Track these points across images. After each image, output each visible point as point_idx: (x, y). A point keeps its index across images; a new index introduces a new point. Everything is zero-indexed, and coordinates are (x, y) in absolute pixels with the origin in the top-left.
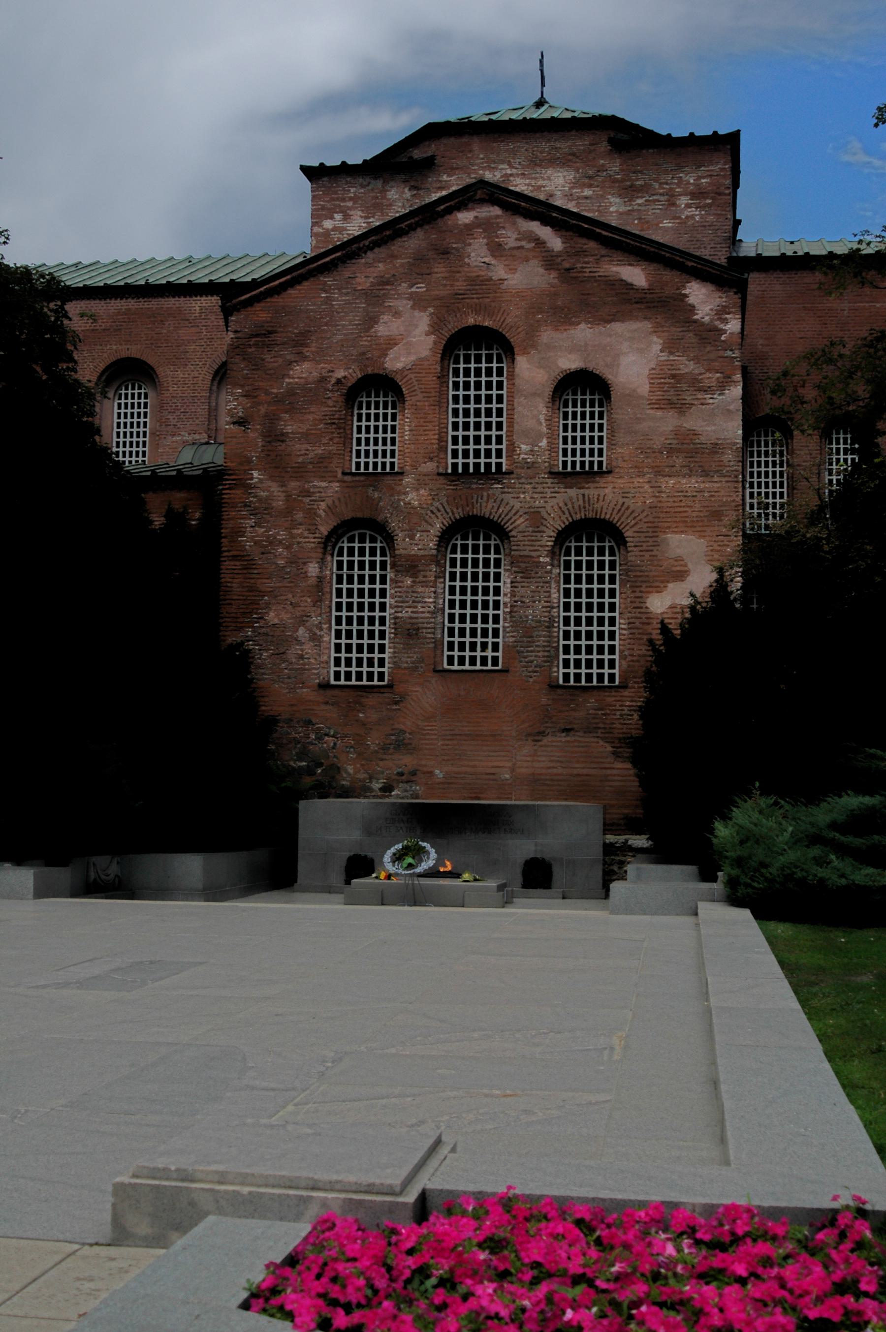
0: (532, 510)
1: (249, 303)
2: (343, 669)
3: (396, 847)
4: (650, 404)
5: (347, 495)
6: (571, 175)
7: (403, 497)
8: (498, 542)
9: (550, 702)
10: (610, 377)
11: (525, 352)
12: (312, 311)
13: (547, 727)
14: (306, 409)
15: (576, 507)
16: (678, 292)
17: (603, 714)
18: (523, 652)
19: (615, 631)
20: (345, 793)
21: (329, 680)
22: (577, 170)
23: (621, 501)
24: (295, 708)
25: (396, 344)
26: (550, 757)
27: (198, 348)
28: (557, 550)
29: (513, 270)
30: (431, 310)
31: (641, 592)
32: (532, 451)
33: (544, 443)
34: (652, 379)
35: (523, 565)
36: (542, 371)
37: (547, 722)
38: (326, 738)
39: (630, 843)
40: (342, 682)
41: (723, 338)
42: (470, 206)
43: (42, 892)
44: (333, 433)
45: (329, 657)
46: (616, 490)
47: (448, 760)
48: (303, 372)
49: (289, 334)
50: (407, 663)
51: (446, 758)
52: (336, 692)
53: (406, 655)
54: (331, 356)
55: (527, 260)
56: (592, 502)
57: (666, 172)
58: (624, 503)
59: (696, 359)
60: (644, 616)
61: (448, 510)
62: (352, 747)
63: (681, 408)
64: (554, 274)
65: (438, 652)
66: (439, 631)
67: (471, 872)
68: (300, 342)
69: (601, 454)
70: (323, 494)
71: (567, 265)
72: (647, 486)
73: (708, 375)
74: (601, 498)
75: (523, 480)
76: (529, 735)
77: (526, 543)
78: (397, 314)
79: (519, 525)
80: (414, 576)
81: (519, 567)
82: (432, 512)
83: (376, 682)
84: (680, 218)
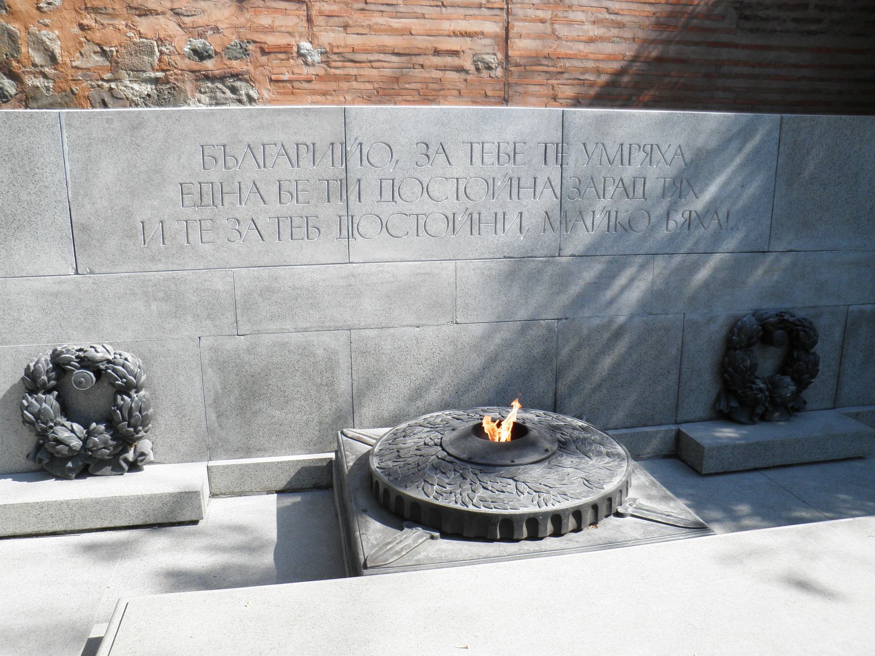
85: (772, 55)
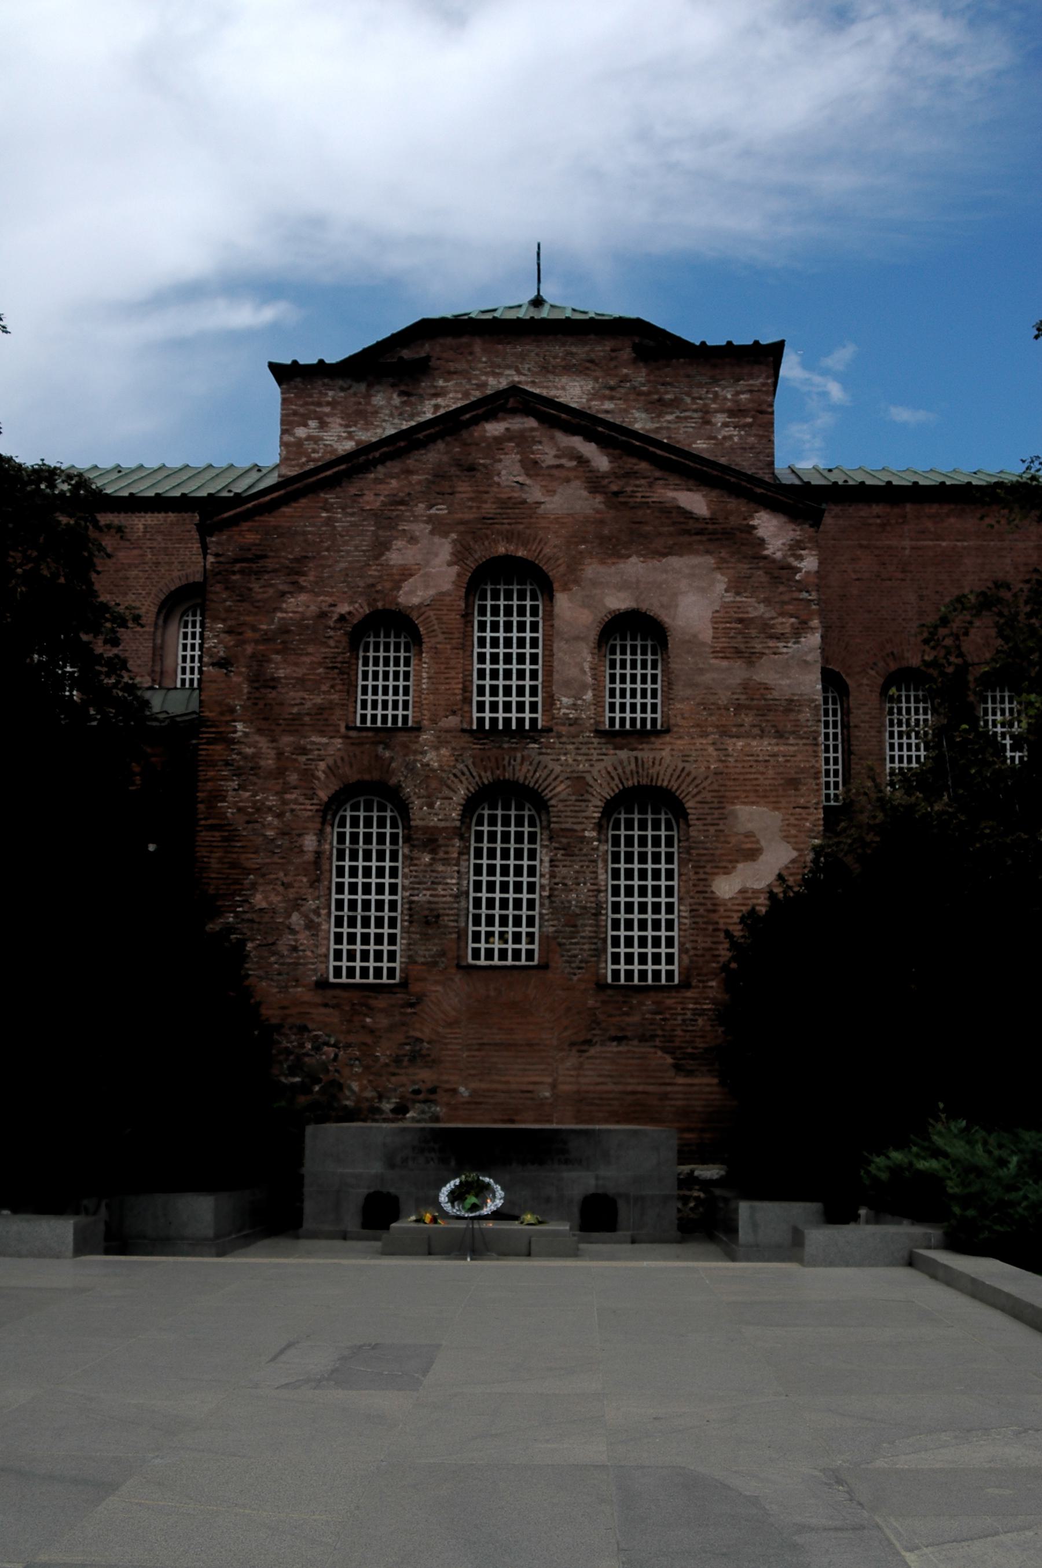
0: (575, 775)
1: (235, 521)
2: (344, 964)
3: (452, 1183)
4: (713, 652)
5: (351, 754)
6: (589, 385)
7: (419, 757)
8: (533, 812)
9: (598, 1005)
10: (666, 619)
11: (566, 588)
12: (310, 533)
13: (595, 1035)
14: (302, 649)
15: (628, 772)
16: (745, 522)
17: (663, 1020)
18: (564, 944)
19: (673, 920)
20: (350, 1115)
21: (328, 978)
22: (596, 379)
23: (681, 765)
24: (287, 1012)
25: (412, 575)
26: (598, 1071)
27: (141, 574)
28: (604, 822)
29: (552, 492)
30: (454, 536)
31: (705, 873)
32: (574, 705)
33: (589, 696)
34: (716, 623)
35: (564, 840)
36: (586, 611)
37: (594, 1029)
38: (326, 1048)
39: (696, 1173)
40: (344, 980)
41: (798, 577)
42: (500, 415)
43: (82, 1247)
44: (334, 679)
45: (328, 949)
46: (674, 753)
47: (474, 1075)
48: (298, 605)
49: (283, 560)
50: (424, 956)
51: (473, 1072)
52: (338, 992)
53: (424, 948)
54: (332, 587)
55: (568, 480)
56: (646, 766)
57: (700, 385)
58: (683, 769)
59: (767, 601)
60: (709, 902)
61: (475, 774)
62: (357, 1059)
63: (750, 658)
64: (599, 498)
65: (462, 944)
66: (463, 919)
67: (533, 1213)
68: (295, 570)
69: (654, 710)
70: (322, 752)
71: (614, 488)
72: (711, 749)
73: (780, 620)
74: (657, 762)
75: (564, 740)
76: (572, 1044)
77: (569, 814)
78: (413, 540)
79: (559, 793)
80: (433, 851)
81: (560, 842)
82: (455, 775)
83: (385, 980)
84: (715, 438)
85: (696, 1088)
